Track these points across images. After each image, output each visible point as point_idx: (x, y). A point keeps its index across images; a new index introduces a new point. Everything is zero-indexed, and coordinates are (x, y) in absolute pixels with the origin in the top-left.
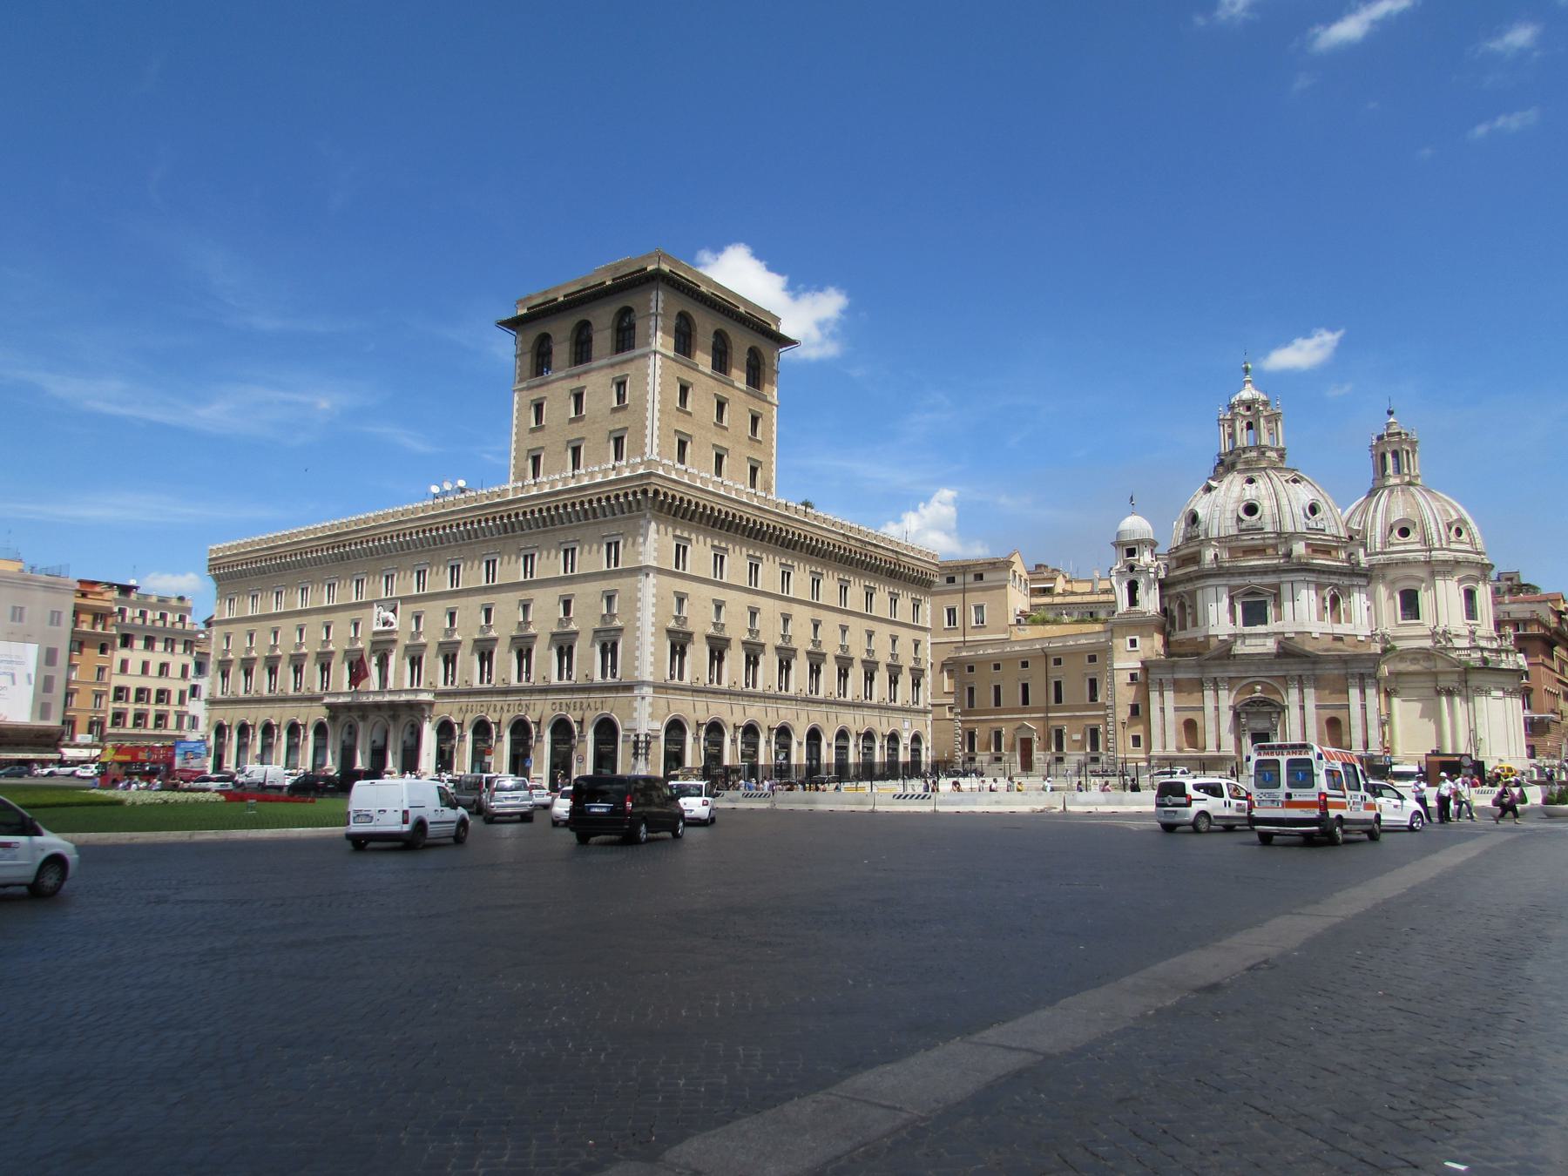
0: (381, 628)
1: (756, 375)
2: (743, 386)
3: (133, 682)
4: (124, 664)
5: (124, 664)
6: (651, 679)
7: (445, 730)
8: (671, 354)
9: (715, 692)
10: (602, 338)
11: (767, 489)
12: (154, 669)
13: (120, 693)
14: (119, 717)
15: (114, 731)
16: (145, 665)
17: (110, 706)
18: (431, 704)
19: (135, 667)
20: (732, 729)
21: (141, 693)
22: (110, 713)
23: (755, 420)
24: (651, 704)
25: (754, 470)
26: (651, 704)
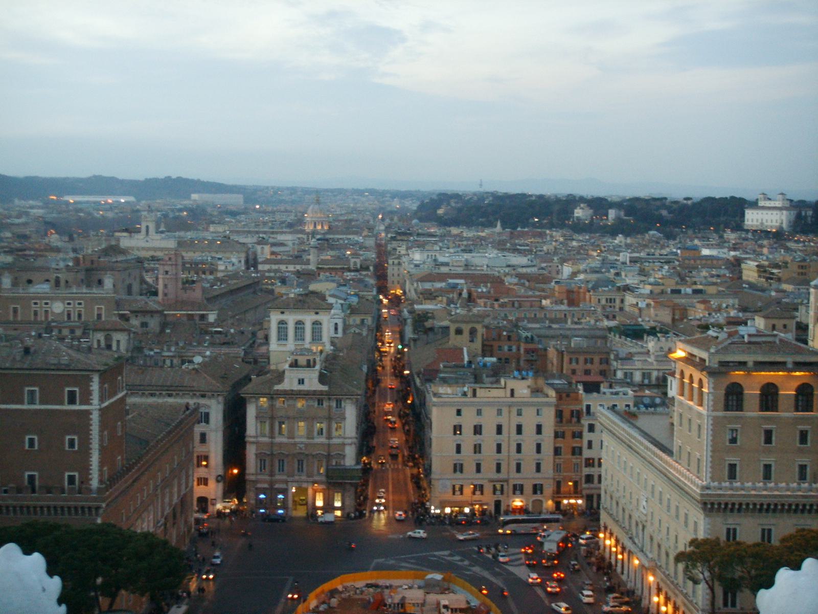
4: (590, 443)
5: (590, 443)
8: (721, 414)
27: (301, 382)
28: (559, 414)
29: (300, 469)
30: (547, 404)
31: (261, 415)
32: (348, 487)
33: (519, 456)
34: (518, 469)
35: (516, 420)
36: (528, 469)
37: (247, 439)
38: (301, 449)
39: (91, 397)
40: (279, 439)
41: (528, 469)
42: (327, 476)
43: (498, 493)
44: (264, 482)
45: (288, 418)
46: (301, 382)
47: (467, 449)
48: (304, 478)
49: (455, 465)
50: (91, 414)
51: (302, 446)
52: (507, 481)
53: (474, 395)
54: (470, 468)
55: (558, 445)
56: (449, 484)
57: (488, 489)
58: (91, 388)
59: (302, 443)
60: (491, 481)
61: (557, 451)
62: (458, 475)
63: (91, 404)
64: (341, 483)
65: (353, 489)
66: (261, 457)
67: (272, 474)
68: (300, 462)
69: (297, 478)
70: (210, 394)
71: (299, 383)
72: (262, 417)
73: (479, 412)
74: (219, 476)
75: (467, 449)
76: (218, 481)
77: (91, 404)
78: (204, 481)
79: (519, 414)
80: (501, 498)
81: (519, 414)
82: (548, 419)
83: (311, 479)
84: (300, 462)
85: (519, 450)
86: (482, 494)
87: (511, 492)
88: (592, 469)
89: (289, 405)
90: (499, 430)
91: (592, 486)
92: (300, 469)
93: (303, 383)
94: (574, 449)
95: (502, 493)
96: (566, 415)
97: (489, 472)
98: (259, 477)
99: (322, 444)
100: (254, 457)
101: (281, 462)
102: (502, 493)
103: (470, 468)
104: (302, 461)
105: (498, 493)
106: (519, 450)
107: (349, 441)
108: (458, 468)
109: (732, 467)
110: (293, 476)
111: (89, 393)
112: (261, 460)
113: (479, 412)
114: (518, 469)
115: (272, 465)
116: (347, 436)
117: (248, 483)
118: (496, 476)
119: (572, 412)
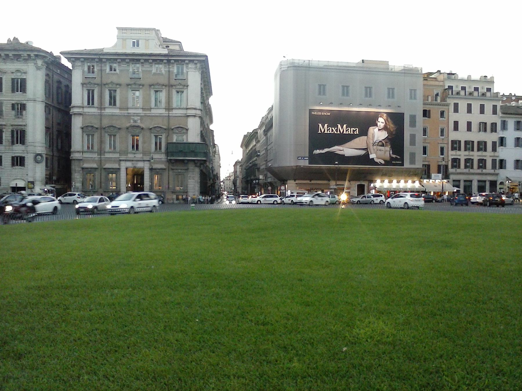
3: (462, 136)
4: (456, 124)
5: (456, 124)
12: (475, 127)
13: (456, 145)
16: (469, 124)
19: (462, 126)
22: (450, 158)
27: (136, 44)
29: (136, 147)
31: (87, 81)
32: (191, 166)
37: (73, 110)
38: (135, 121)
40: (110, 111)
42: (167, 153)
44: (93, 160)
45: (120, 85)
48: (139, 156)
51: (136, 118)
59: (137, 115)
64: (183, 160)
65: (197, 170)
67: (101, 152)
69: (131, 156)
70: (25, 54)
71: (134, 45)
72: (90, 83)
76: (37, 162)
78: (19, 161)
88: (458, 153)
89: (121, 71)
91: (458, 171)
93: (138, 46)
98: (86, 155)
99: (160, 116)
100: (80, 131)
107: (193, 112)
110: (126, 153)
112: (88, 135)
115: (101, 142)
116: (189, 107)
117: (73, 162)
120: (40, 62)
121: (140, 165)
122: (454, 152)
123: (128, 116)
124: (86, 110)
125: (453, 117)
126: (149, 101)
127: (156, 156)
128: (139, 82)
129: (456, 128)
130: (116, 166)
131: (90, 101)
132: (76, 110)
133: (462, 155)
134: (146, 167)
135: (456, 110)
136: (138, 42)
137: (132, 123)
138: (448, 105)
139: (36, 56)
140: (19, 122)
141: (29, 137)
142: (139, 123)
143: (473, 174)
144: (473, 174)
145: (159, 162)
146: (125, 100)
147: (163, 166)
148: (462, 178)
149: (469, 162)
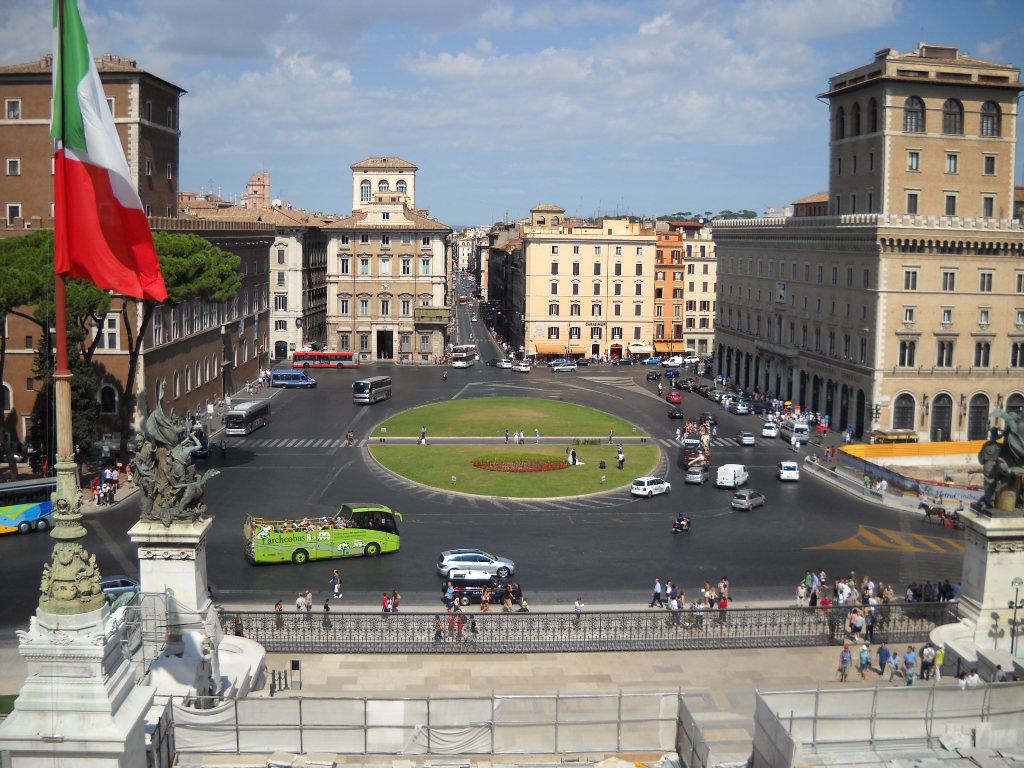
0: (778, 299)
1: (993, 119)
2: (976, 137)
3: (698, 296)
4: (692, 285)
5: (692, 285)
6: (882, 368)
7: (804, 377)
8: (899, 133)
9: (943, 375)
10: (865, 117)
11: (1002, 214)
13: (691, 305)
14: (691, 322)
15: (688, 330)
16: (705, 284)
17: (686, 314)
18: (797, 358)
19: (698, 287)
20: (959, 400)
21: (704, 305)
22: (685, 318)
23: (990, 161)
24: (882, 385)
25: (989, 201)
26: (882, 385)
27: (386, 216)
28: (659, 255)
29: (385, 310)
30: (648, 243)
33: (618, 298)
34: (617, 312)
35: (614, 260)
36: (628, 310)
38: (385, 288)
39: (129, 108)
41: (628, 310)
43: (596, 337)
44: (347, 324)
45: (372, 256)
46: (386, 216)
47: (565, 288)
49: (551, 306)
50: (130, 128)
52: (605, 324)
53: (570, 232)
54: (565, 309)
55: (658, 287)
56: (545, 327)
57: (586, 331)
58: (130, 97)
60: (588, 323)
61: (659, 293)
62: (554, 317)
63: (129, 116)
66: (344, 298)
67: (354, 317)
68: (385, 303)
69: (381, 320)
73: (576, 250)
74: (298, 319)
75: (565, 288)
76: (297, 325)
77: (129, 116)
78: (281, 325)
79: (618, 253)
80: (599, 342)
81: (618, 252)
82: (648, 256)
83: (396, 321)
84: (385, 303)
85: (618, 290)
86: (579, 338)
87: (610, 336)
88: (693, 313)
90: (597, 269)
91: (693, 330)
92: (385, 310)
94: (675, 291)
95: (600, 338)
96: (667, 253)
97: (586, 313)
98: (340, 319)
101: (365, 303)
102: (600, 338)
103: (565, 309)
104: (387, 302)
105: (596, 337)
106: (618, 290)
107: (438, 280)
108: (554, 309)
109: (913, 198)
111: (128, 102)
113: (576, 250)
114: (617, 312)
118: (593, 318)
119: (673, 253)
120: (300, 235)
121: (389, 328)
122: (689, 313)
123: (379, 283)
124: (341, 278)
125: (688, 278)
126: (398, 270)
127: (404, 320)
128: (388, 252)
129: (692, 288)
130: (368, 329)
131: (345, 269)
132: (332, 279)
133: (697, 315)
134: (395, 329)
135: (691, 270)
136: (388, 214)
137: (382, 290)
138: (683, 267)
139: (297, 231)
140: (281, 290)
141: (290, 304)
142: (388, 290)
143: (707, 333)
144: (707, 333)
145: (407, 324)
146: (376, 268)
147: (410, 329)
148: (697, 337)
149: (704, 322)
